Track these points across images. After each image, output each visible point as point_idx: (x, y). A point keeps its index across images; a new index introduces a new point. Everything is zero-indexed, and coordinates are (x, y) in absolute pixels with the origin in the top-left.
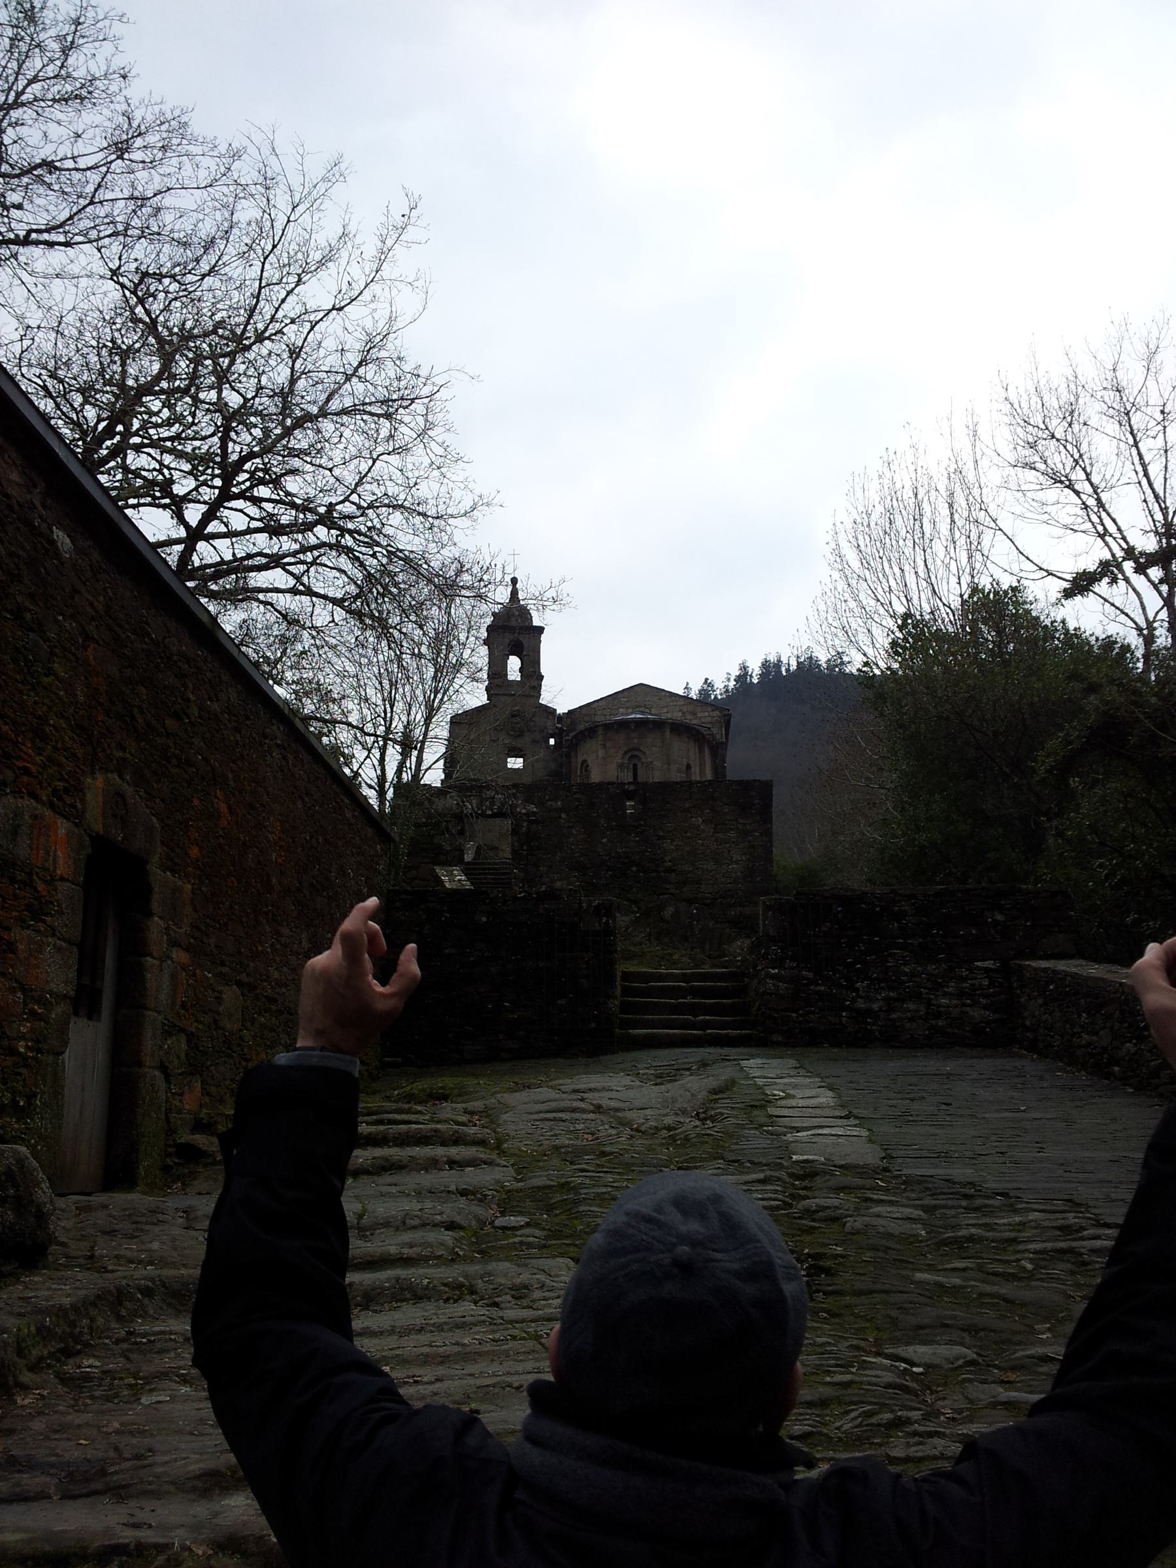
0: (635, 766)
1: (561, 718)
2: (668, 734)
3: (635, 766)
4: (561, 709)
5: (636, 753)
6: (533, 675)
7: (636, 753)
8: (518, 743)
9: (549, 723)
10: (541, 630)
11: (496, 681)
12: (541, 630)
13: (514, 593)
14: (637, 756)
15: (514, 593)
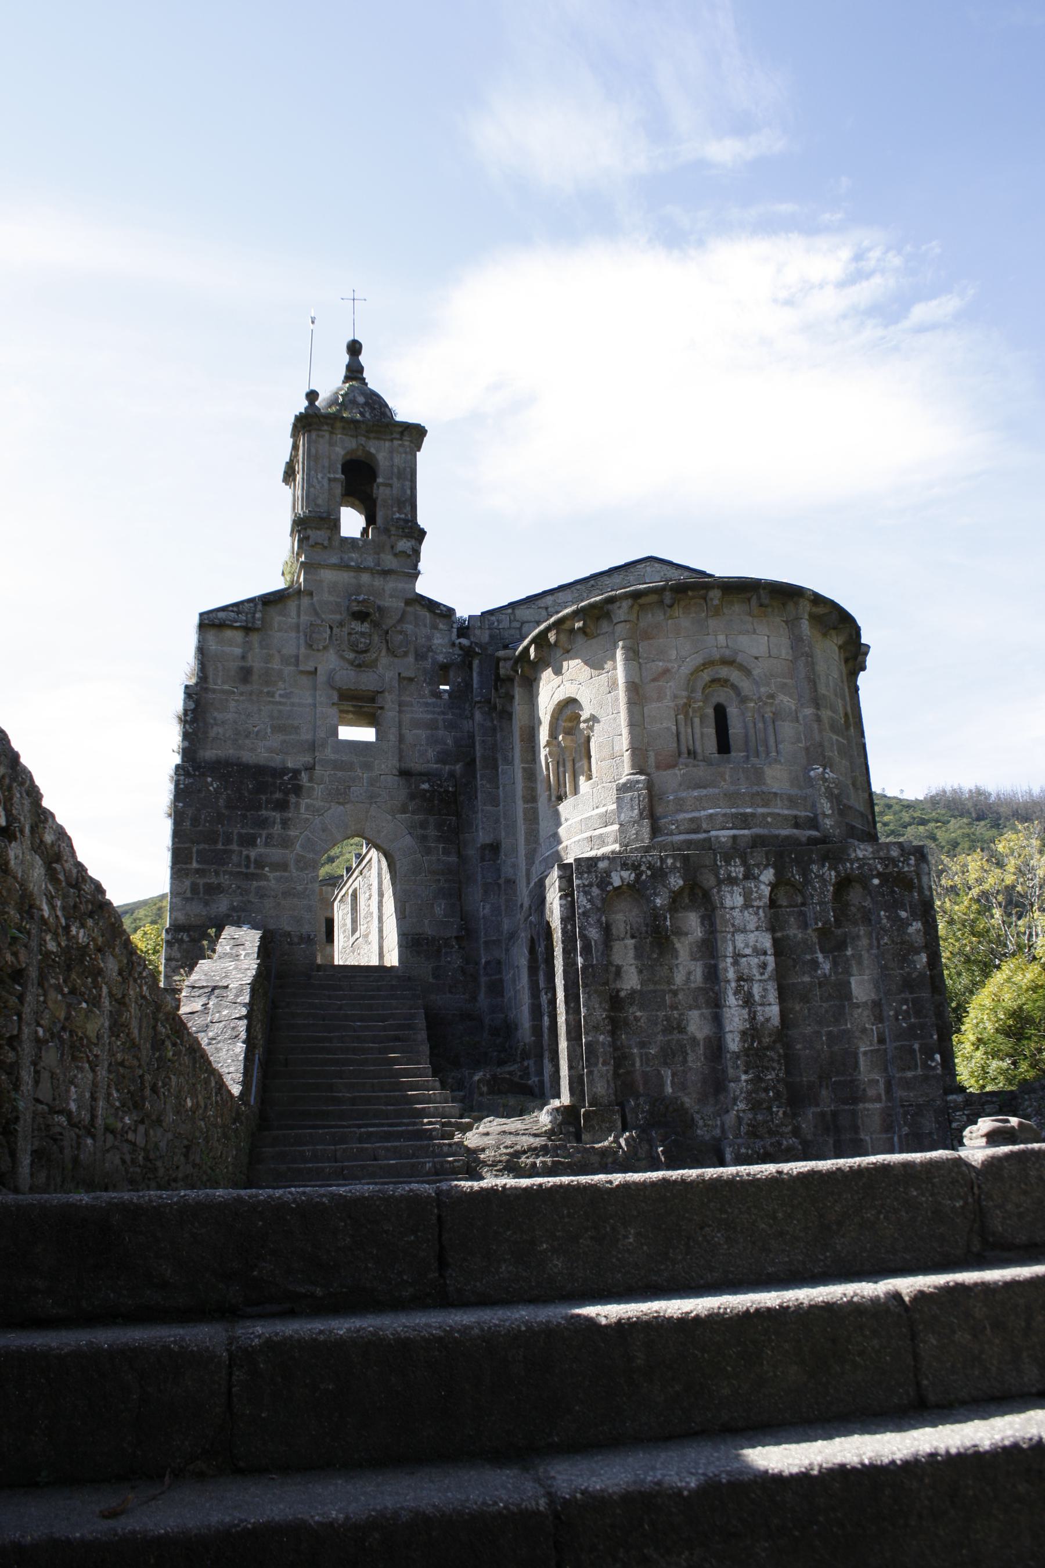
0: (720, 713)
1: (465, 629)
2: (805, 625)
3: (720, 713)
4: (466, 608)
5: (724, 672)
6: (400, 532)
7: (724, 672)
8: (367, 681)
9: (438, 640)
10: (415, 433)
11: (318, 535)
12: (415, 433)
13: (354, 372)
14: (724, 682)
15: (354, 372)
